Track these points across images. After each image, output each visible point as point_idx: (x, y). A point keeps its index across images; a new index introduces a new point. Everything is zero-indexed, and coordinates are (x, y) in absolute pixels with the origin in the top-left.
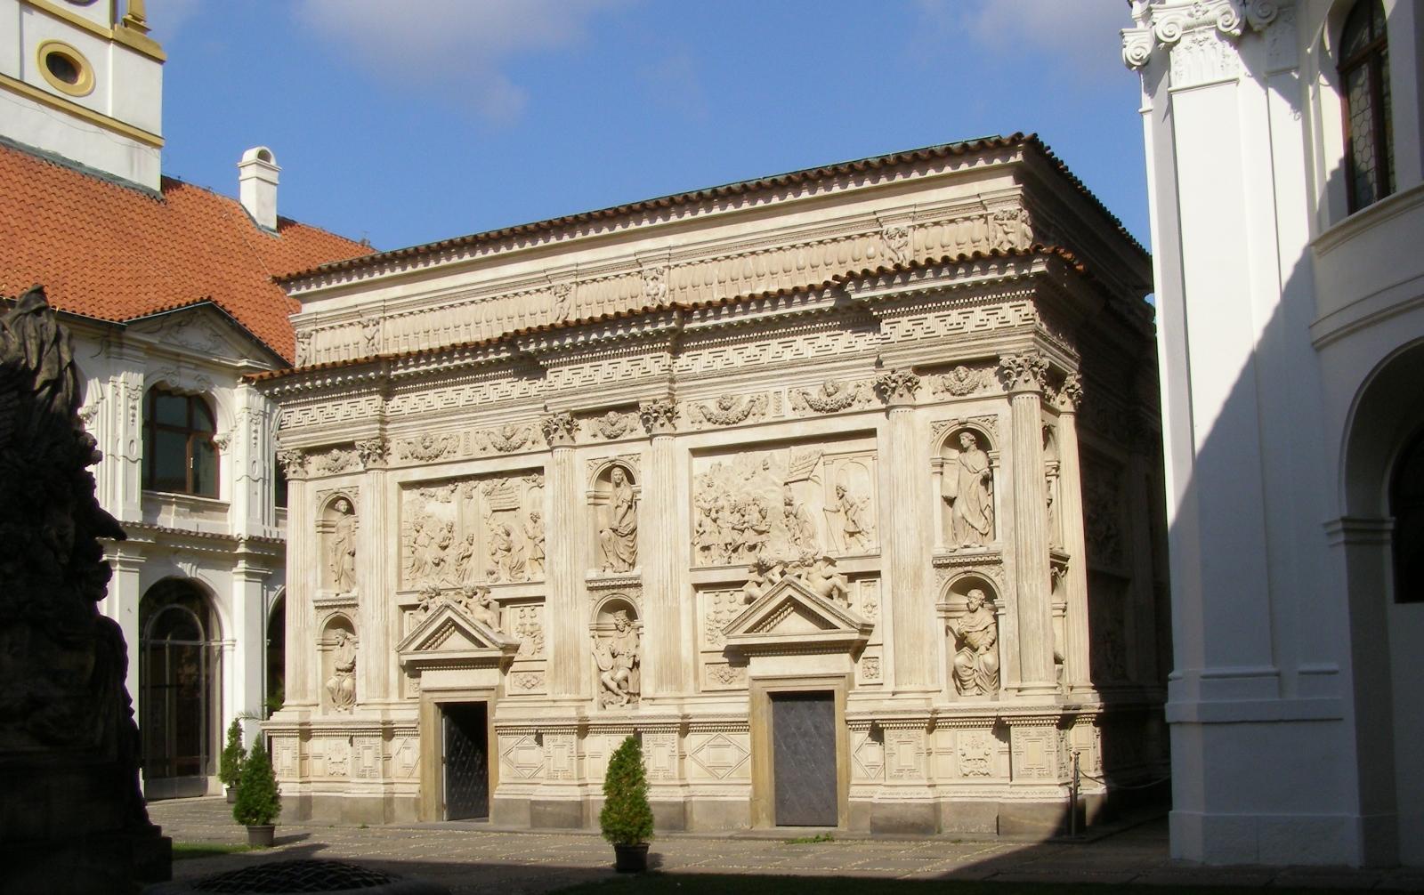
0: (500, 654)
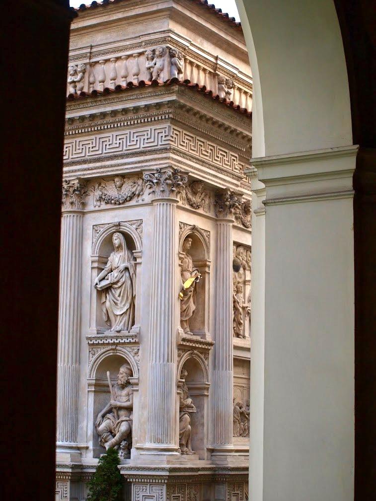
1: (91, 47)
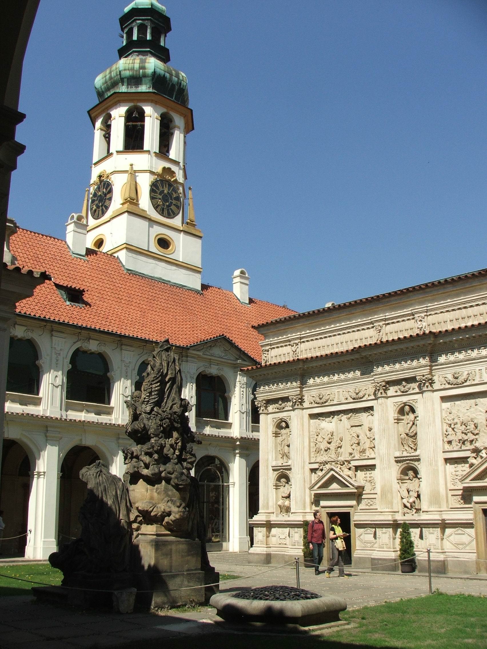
0: (356, 491)
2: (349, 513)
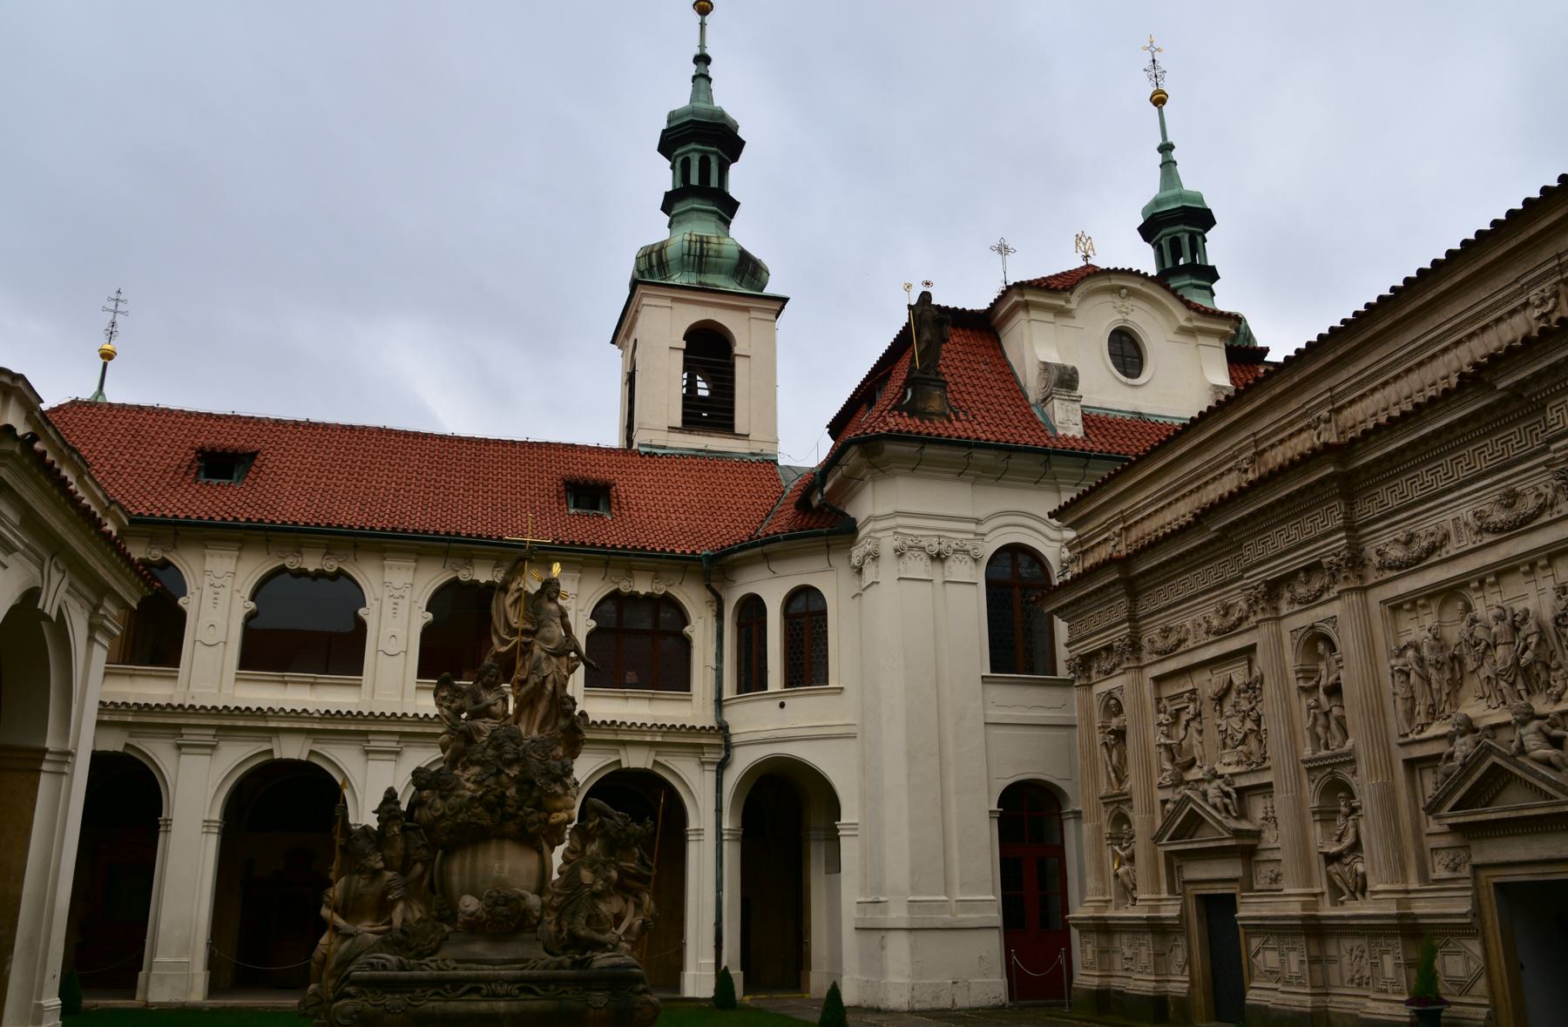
0: (1233, 843)
1: (1559, 256)
2: (1234, 895)
